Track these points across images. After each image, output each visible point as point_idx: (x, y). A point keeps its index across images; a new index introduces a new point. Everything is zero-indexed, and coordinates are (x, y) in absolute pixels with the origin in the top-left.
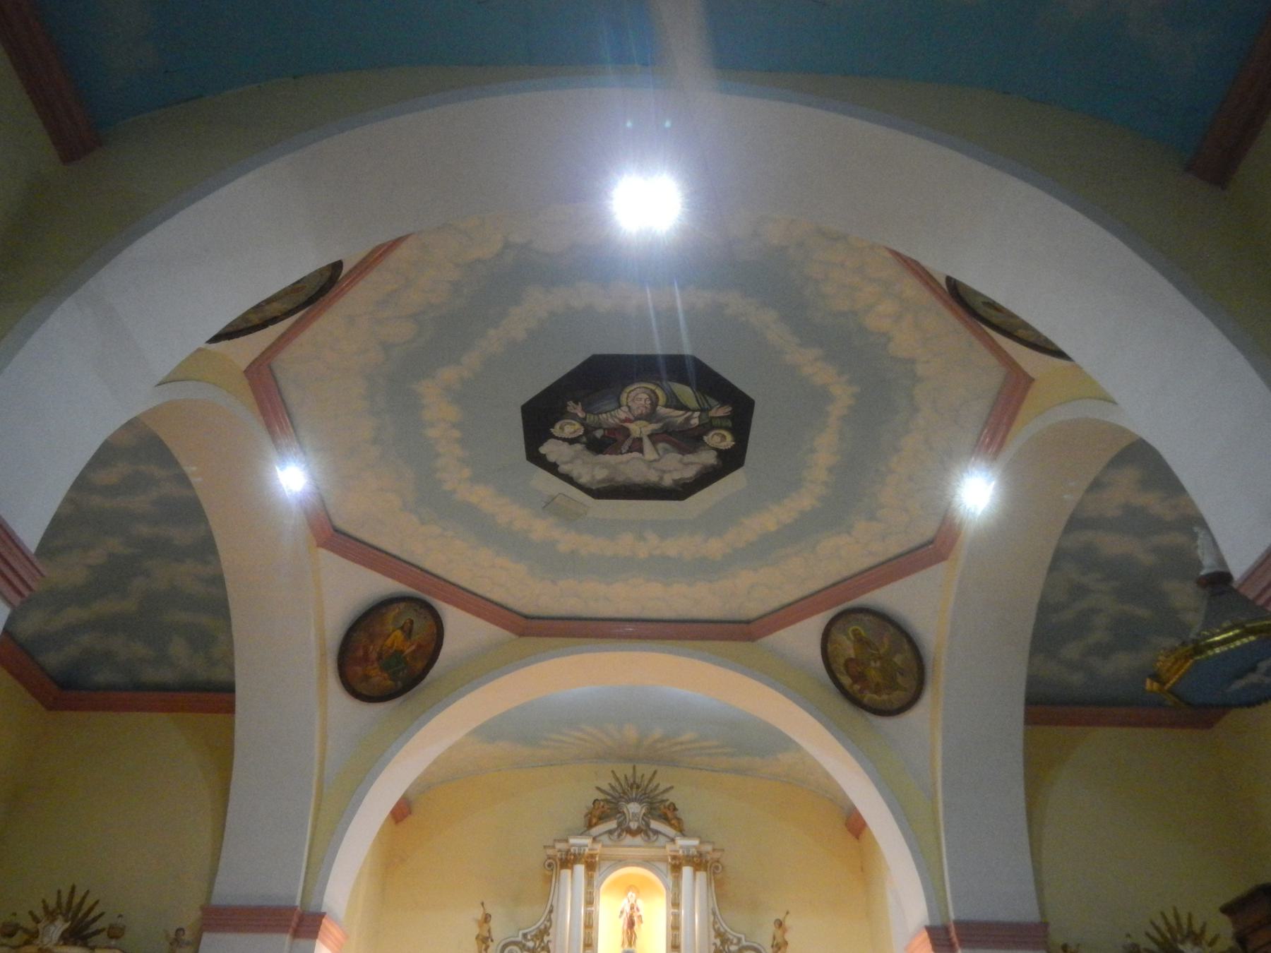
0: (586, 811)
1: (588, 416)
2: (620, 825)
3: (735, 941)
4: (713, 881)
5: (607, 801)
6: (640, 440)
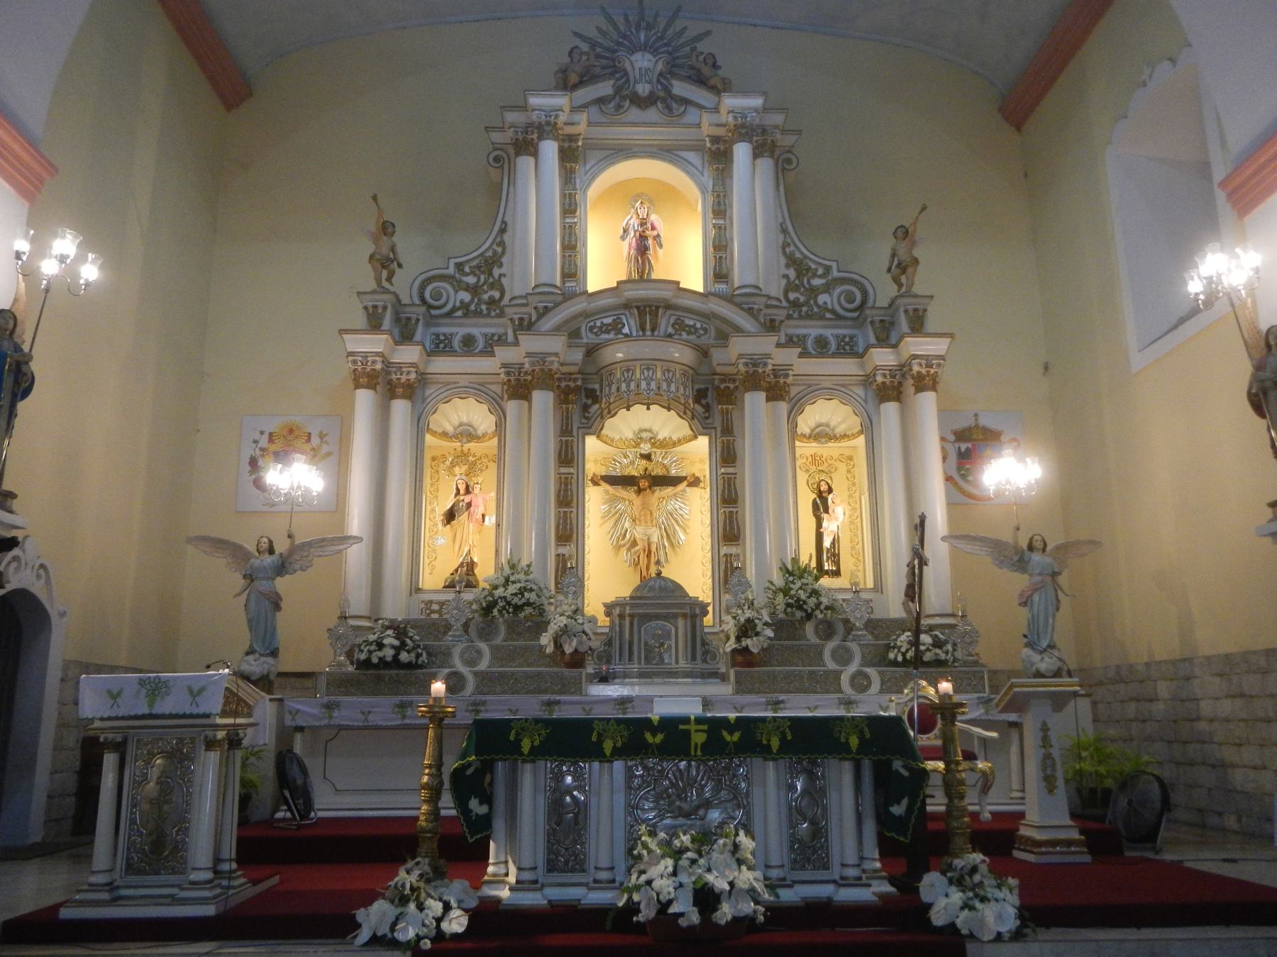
0: (557, 68)
2: (618, 90)
3: (820, 272)
4: (781, 181)
5: (598, 56)
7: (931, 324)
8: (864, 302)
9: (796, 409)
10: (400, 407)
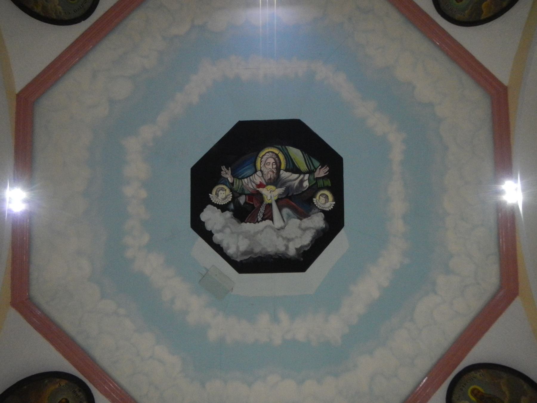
1: (235, 181)
6: (270, 205)
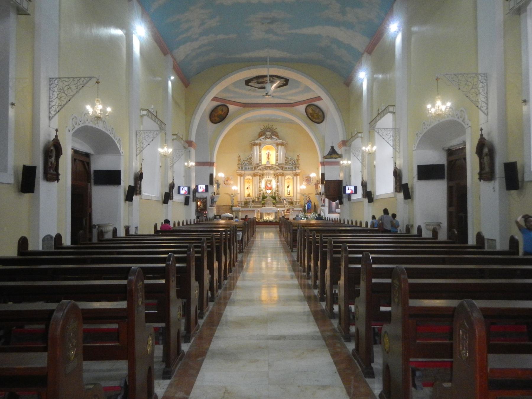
2: (265, 137)
5: (262, 132)
7: (300, 168)
8: (294, 162)
9: (285, 176)
10: (242, 178)
